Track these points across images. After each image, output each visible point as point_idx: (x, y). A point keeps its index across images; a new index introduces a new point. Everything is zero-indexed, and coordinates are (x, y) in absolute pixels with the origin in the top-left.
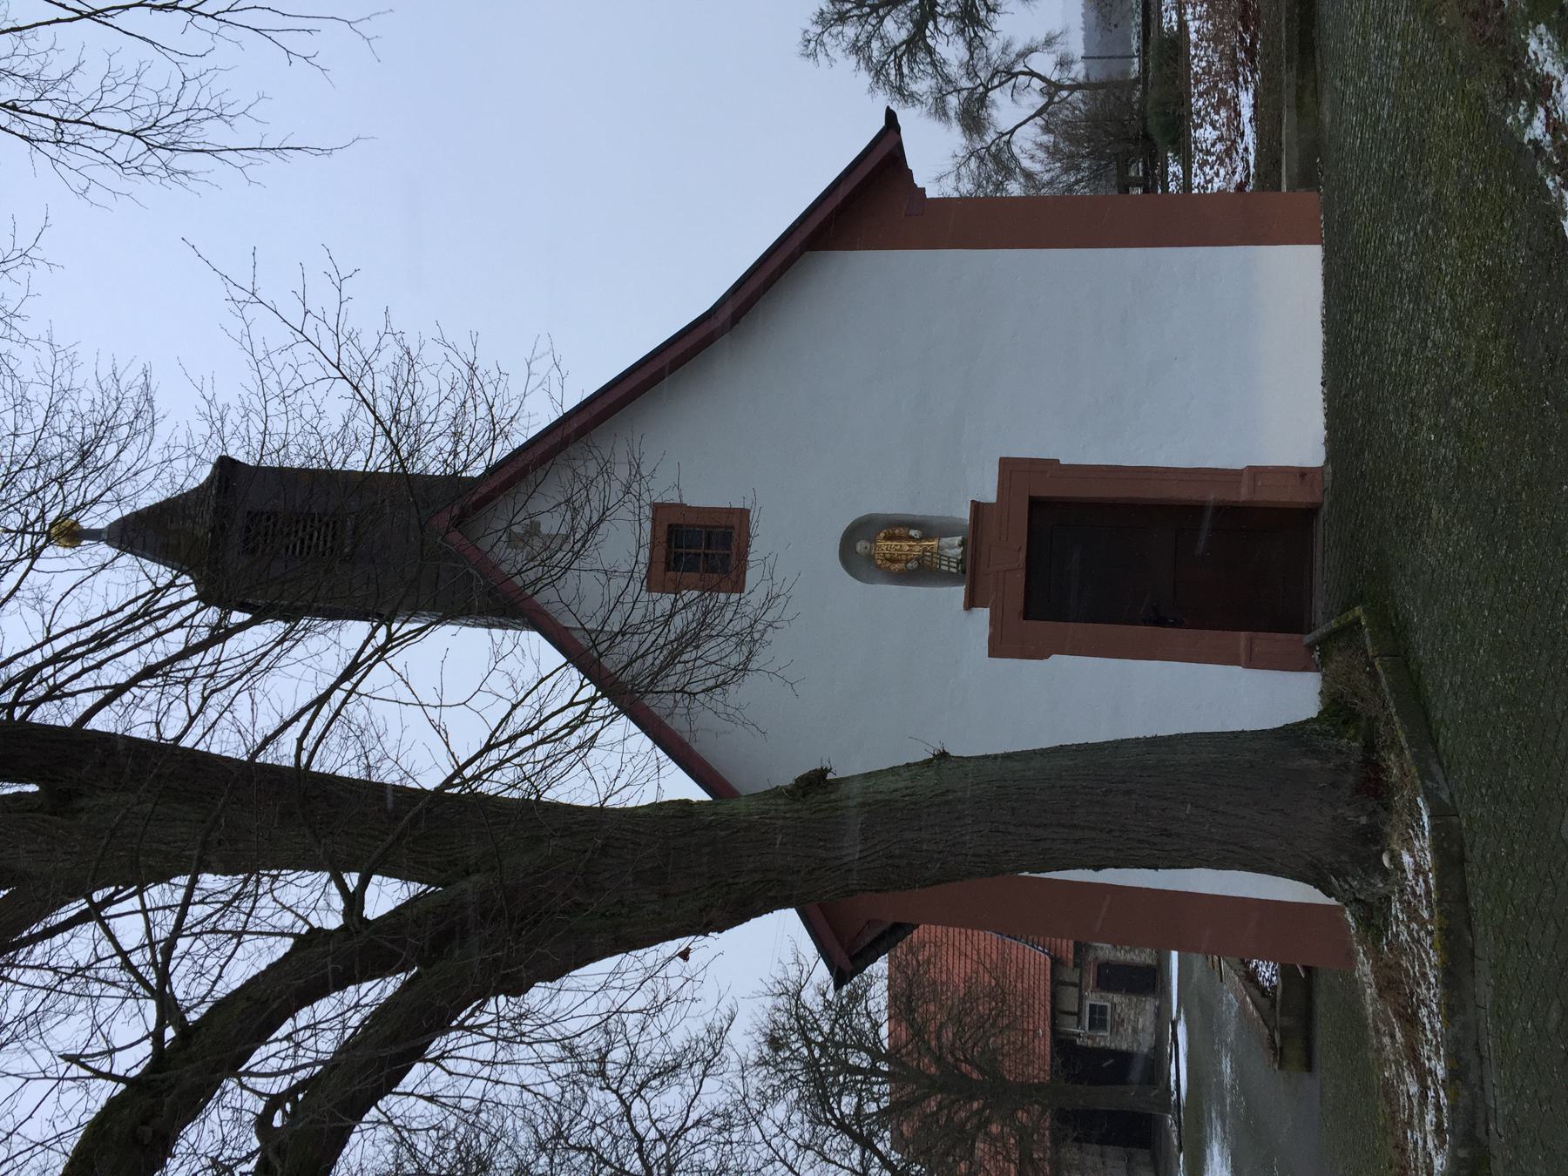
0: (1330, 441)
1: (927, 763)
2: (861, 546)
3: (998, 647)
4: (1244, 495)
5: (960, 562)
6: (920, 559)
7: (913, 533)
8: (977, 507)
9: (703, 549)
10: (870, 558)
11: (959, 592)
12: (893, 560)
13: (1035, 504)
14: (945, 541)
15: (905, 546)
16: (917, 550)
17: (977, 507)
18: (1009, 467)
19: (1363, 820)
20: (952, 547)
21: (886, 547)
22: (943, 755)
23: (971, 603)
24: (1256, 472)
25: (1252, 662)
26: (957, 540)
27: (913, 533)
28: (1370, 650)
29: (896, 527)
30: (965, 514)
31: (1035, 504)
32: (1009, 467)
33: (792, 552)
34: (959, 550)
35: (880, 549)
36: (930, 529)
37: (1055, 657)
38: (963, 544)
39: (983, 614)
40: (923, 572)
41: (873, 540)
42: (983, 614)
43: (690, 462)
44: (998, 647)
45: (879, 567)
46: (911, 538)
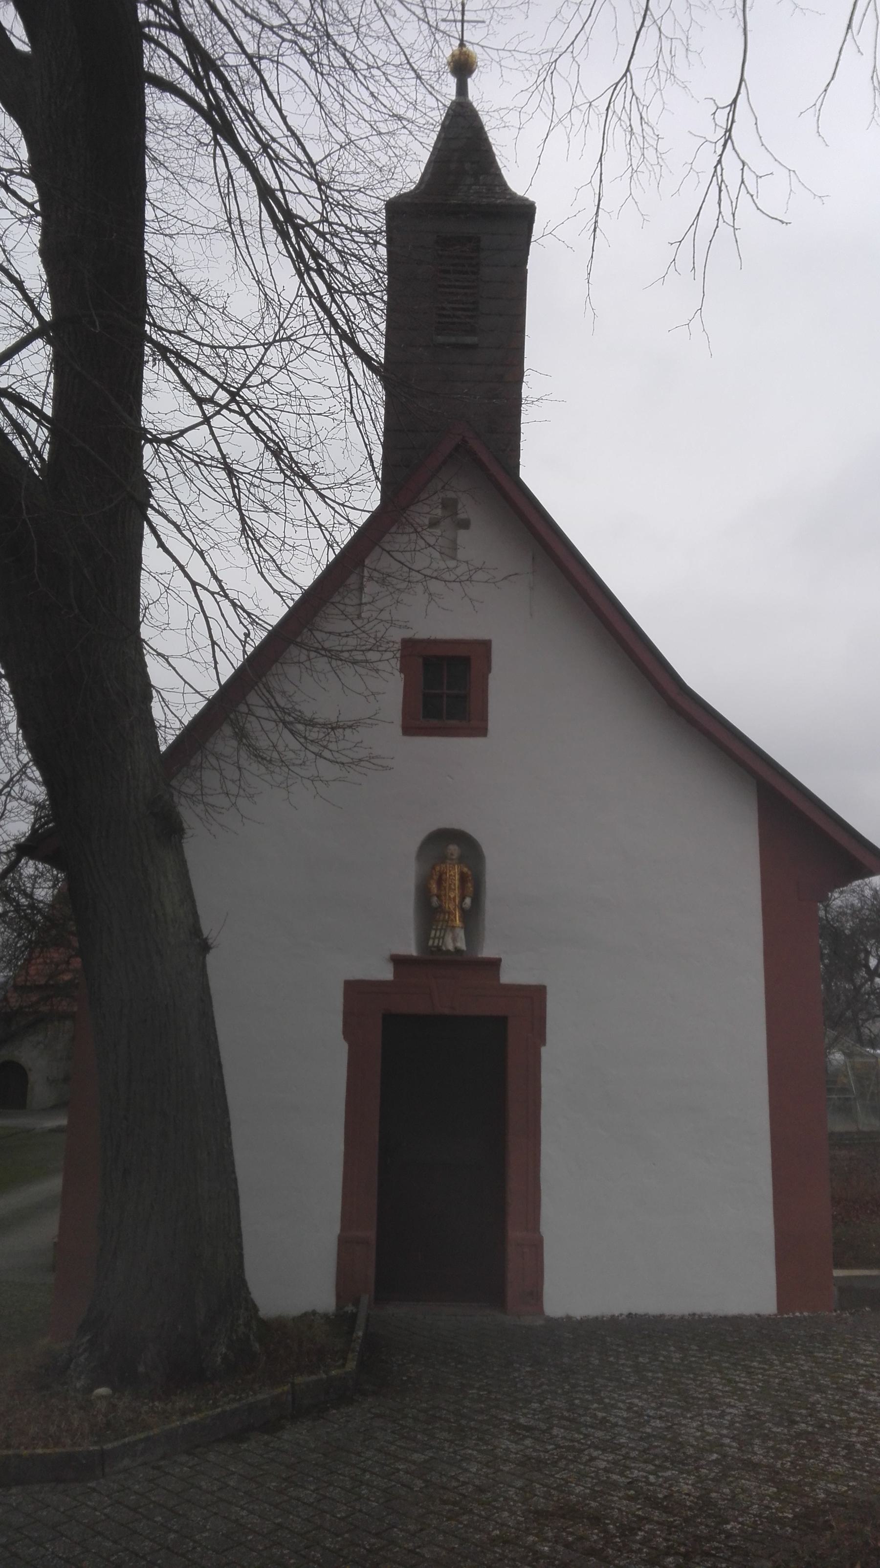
0: (568, 1323)
1: (196, 930)
2: (454, 849)
3: (357, 992)
4: (515, 1234)
5: (439, 948)
6: (440, 909)
7: (468, 901)
8: (494, 964)
9: (447, 689)
10: (443, 858)
11: (411, 949)
12: (440, 882)
13: (501, 1022)
14: (461, 934)
15: (455, 894)
16: (450, 906)
17: (494, 964)
18: (535, 996)
19: (141, 1369)
20: (455, 940)
21: (454, 873)
22: (205, 947)
23: (398, 961)
24: (537, 1246)
25: (345, 1243)
26: (462, 945)
27: (468, 901)
28: (299, 1380)
29: (474, 883)
30: (488, 951)
31: (501, 1022)
32: (535, 996)
33: (455, 781)
34: (451, 947)
35: (452, 865)
36: (472, 918)
37: (345, 1046)
38: (458, 951)
39: (386, 973)
40: (430, 912)
41: (461, 860)
42: (386, 973)
43: (533, 674)
44: (357, 992)
45: (433, 868)
46: (463, 898)
